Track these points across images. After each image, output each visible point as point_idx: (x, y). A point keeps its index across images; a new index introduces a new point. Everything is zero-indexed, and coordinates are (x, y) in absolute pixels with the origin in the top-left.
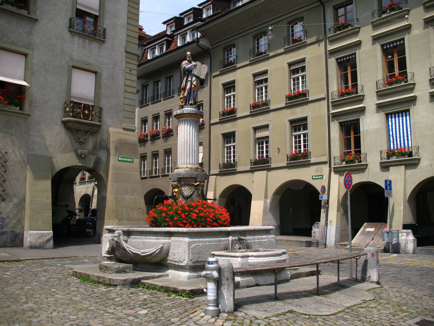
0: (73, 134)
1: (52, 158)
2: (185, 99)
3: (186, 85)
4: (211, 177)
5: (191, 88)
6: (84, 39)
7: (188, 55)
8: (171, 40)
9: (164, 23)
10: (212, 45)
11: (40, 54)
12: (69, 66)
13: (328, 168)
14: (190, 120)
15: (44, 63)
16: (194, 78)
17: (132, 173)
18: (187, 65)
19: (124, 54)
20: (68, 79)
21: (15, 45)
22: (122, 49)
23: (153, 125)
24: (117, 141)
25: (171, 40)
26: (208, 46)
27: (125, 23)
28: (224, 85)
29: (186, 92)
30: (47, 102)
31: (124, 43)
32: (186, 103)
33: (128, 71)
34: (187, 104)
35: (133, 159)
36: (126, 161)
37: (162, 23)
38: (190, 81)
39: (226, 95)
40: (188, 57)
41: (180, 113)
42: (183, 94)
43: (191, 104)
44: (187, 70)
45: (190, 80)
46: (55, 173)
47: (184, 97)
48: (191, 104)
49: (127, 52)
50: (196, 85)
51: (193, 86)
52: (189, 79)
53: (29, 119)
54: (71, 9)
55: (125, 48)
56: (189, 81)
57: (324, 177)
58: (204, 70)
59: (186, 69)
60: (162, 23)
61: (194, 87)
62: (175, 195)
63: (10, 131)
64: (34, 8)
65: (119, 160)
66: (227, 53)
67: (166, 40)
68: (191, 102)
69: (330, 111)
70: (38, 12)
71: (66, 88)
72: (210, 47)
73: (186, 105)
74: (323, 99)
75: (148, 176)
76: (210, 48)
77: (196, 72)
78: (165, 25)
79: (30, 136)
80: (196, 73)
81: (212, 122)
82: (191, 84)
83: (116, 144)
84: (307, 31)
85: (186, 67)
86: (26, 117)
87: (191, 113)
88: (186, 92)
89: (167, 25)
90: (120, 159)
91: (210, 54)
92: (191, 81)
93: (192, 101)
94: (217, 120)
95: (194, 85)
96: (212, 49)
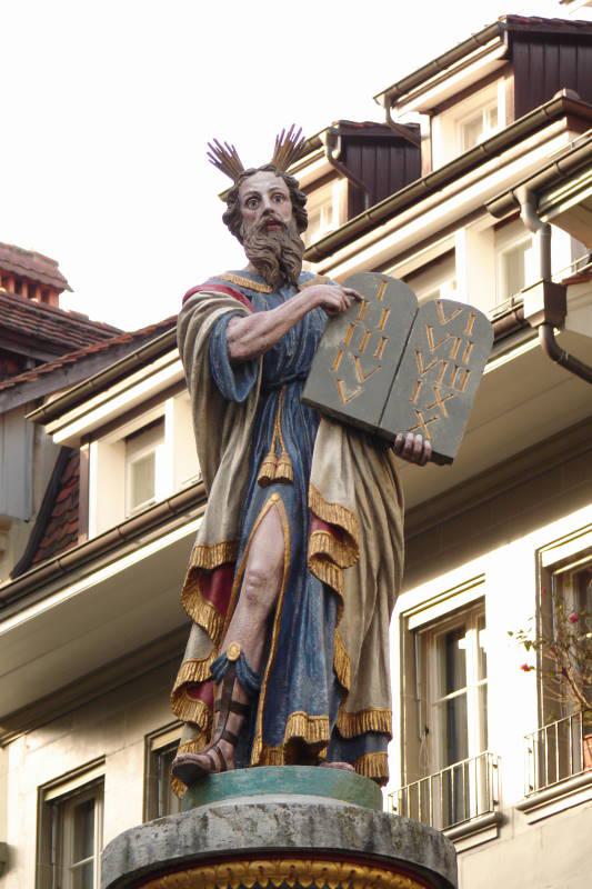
2: (236, 694)
3: (237, 543)
5: (296, 566)
7: (256, 198)
16: (330, 452)
18: (241, 314)
29: (246, 620)
32: (241, 741)
34: (258, 747)
38: (282, 480)
40: (259, 221)
41: (161, 856)
42: (218, 636)
43: (302, 753)
44: (241, 366)
45: (284, 471)
47: (225, 672)
48: (302, 753)
50: (349, 525)
51: (319, 542)
52: (276, 466)
56: (267, 483)
58: (443, 353)
59: (238, 350)
61: (328, 550)
68: (296, 726)
73: (242, 759)
77: (352, 384)
80: (348, 398)
82: (302, 518)
85: (237, 325)
87: (299, 841)
88: (246, 620)
92: (297, 486)
93: (308, 710)
95: (338, 533)
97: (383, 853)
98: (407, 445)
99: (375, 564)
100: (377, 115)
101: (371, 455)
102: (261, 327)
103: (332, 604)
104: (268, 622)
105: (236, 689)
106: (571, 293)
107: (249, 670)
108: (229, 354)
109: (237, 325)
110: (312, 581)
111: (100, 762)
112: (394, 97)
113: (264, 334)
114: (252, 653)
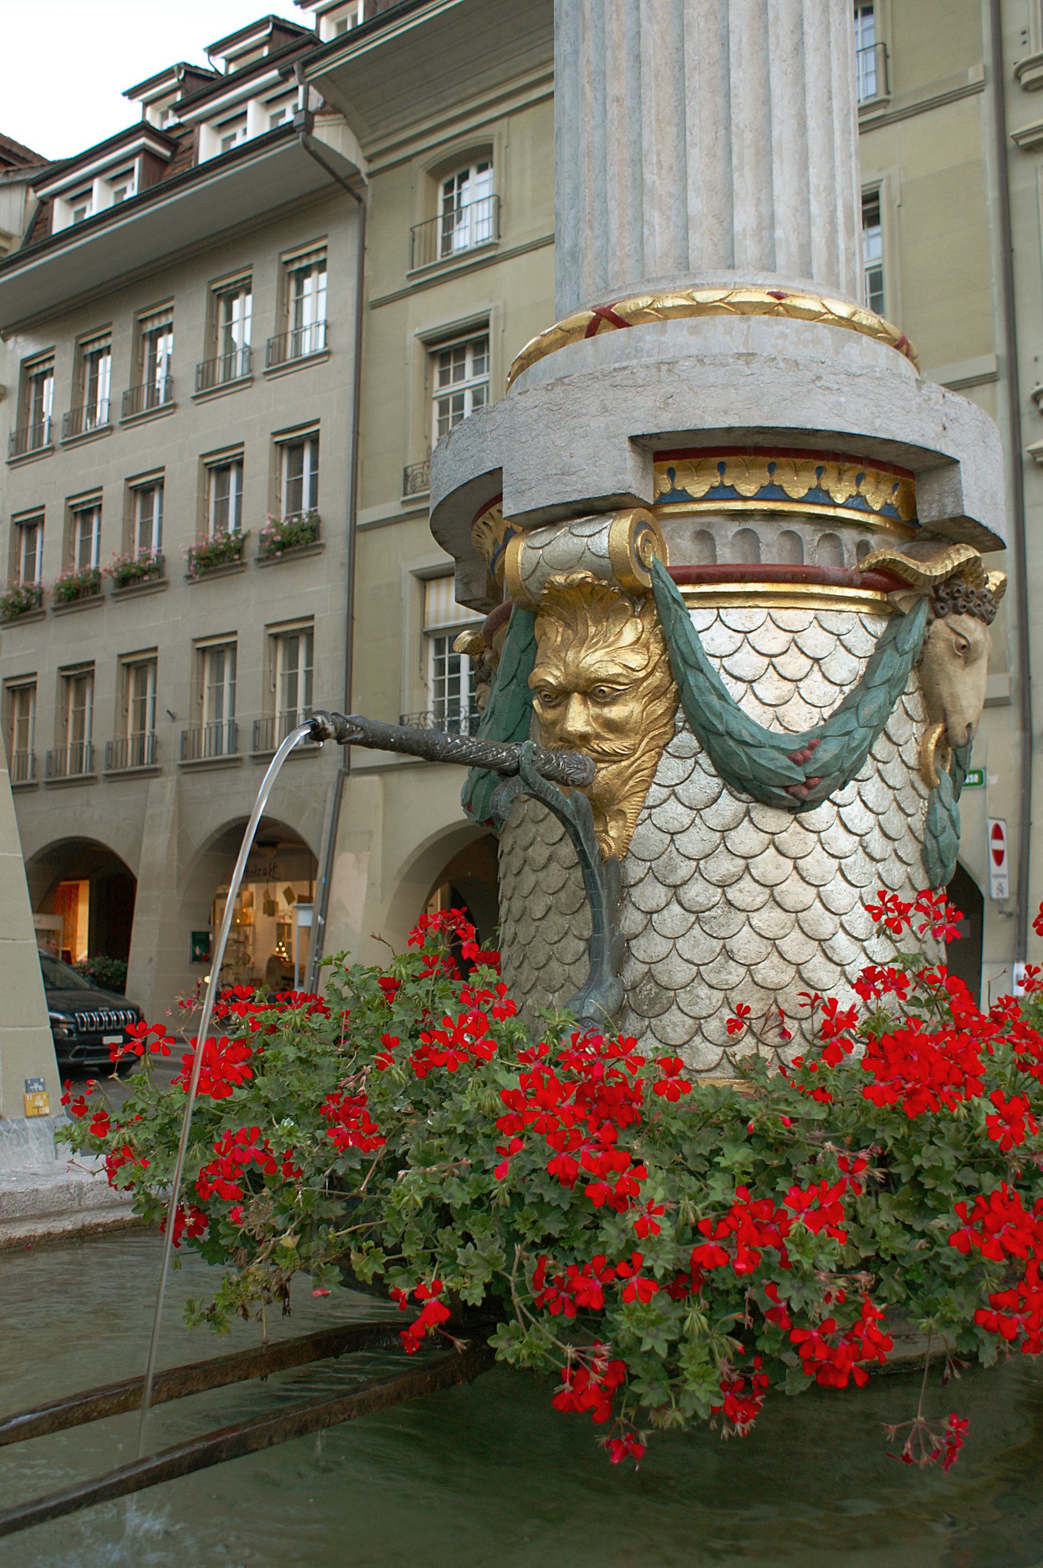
4: (354, 782)
8: (167, 153)
9: (132, 93)
10: (370, 160)
13: (1015, 736)
23: (69, 543)
25: (167, 153)
26: (353, 161)
28: (429, 342)
37: (124, 94)
39: (438, 390)
57: (992, 780)
60: (124, 94)
62: (584, 738)
66: (446, 193)
67: (144, 150)
69: (1024, 442)
72: (364, 168)
74: (990, 378)
75: (42, 779)
76: (358, 172)
78: (137, 104)
81: (365, 517)
84: (890, 52)
89: (146, 104)
91: (359, 199)
94: (392, 508)
96: (370, 175)
100: (202, 61)
106: (317, 118)
111: (52, 349)
112: (213, 50)
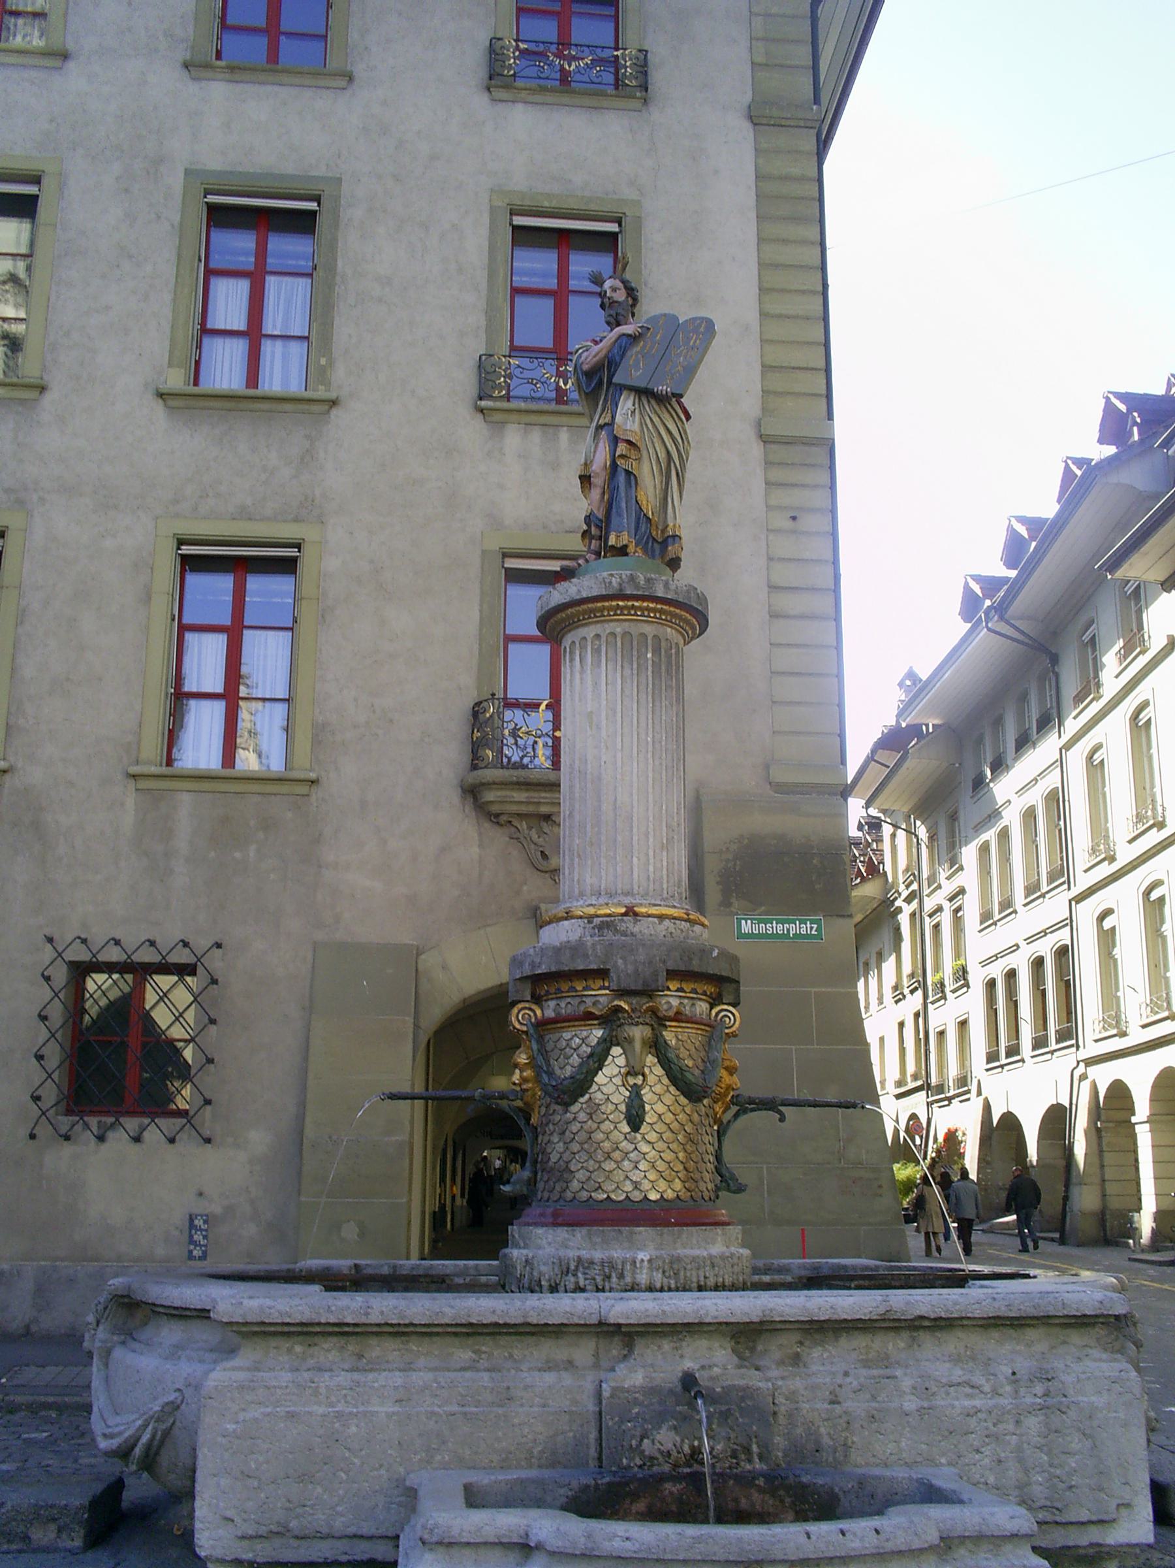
0: (518, 839)
1: (418, 955)
6: (551, 430)
11: (351, 533)
12: (483, 552)
14: (598, 636)
15: (372, 562)
17: (813, 990)
19: (756, 450)
20: (481, 611)
21: (250, 519)
22: (750, 434)
24: (734, 847)
27: (752, 316)
30: (391, 721)
31: (751, 405)
33: (783, 522)
35: (818, 922)
36: (786, 936)
38: (606, 424)
46: (435, 1015)
49: (766, 439)
53: (313, 798)
54: (483, 322)
55: (759, 424)
59: (585, 367)
63: (238, 855)
64: (323, 361)
65: (741, 935)
70: (340, 374)
71: (476, 647)
79: (320, 866)
83: (728, 861)
86: (302, 789)
90: (746, 927)
97: (628, 592)
98: (664, 392)
99: (662, 455)
101: (653, 402)
102: (594, 353)
103: (632, 478)
104: (604, 493)
105: (593, 529)
107: (597, 518)
108: (581, 369)
109: (585, 354)
110: (619, 469)
113: (595, 357)
114: (599, 510)
